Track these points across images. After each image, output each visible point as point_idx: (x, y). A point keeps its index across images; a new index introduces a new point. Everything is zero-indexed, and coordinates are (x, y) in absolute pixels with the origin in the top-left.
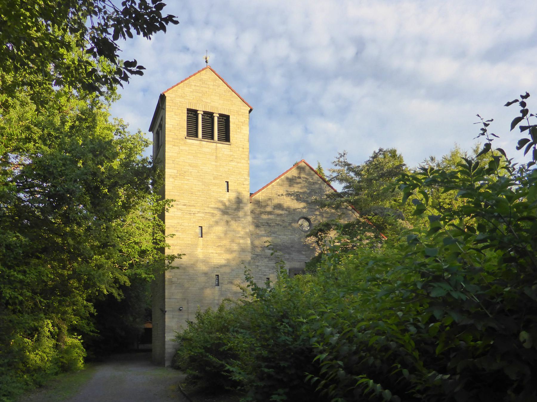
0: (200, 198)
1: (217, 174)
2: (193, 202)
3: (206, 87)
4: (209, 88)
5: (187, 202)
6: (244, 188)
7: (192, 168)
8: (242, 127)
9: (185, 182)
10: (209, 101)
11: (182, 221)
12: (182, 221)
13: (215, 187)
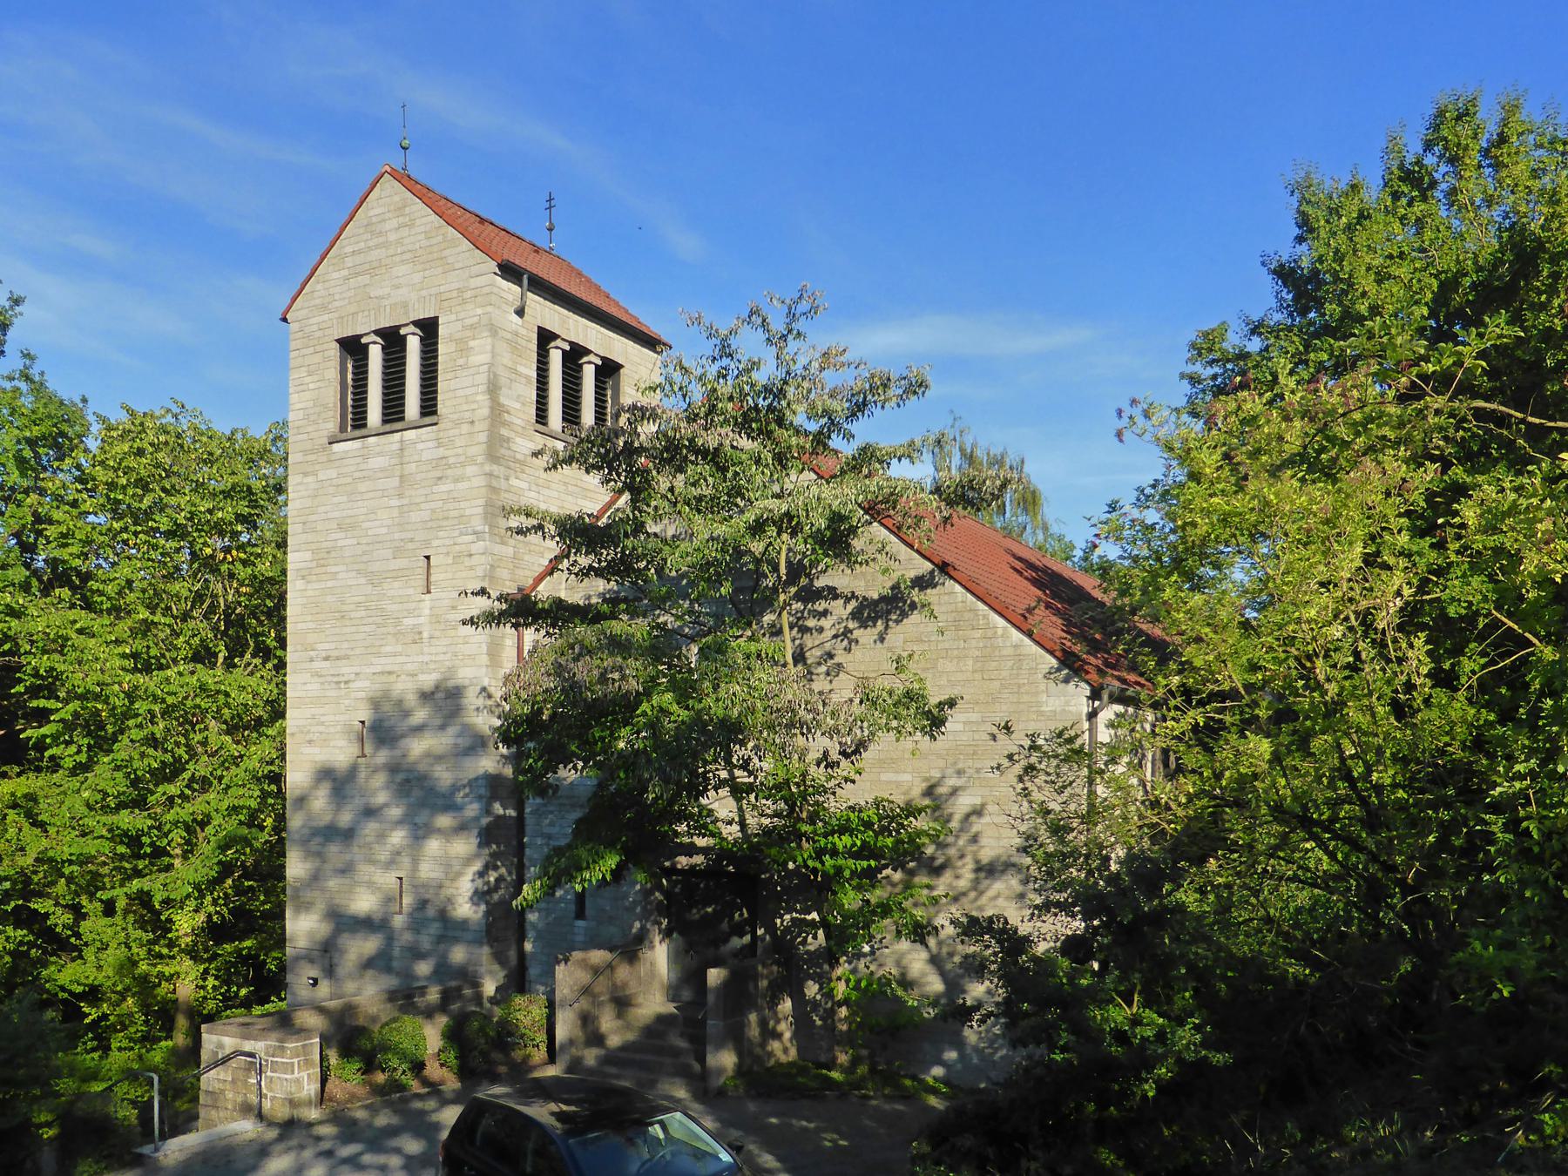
0: (362, 629)
1: (403, 535)
2: (345, 645)
3: (377, 247)
4: (386, 245)
5: (333, 646)
6: (471, 568)
7: (342, 535)
8: (472, 343)
9: (330, 584)
10: (387, 290)
11: (322, 711)
12: (322, 711)
13: (396, 585)
